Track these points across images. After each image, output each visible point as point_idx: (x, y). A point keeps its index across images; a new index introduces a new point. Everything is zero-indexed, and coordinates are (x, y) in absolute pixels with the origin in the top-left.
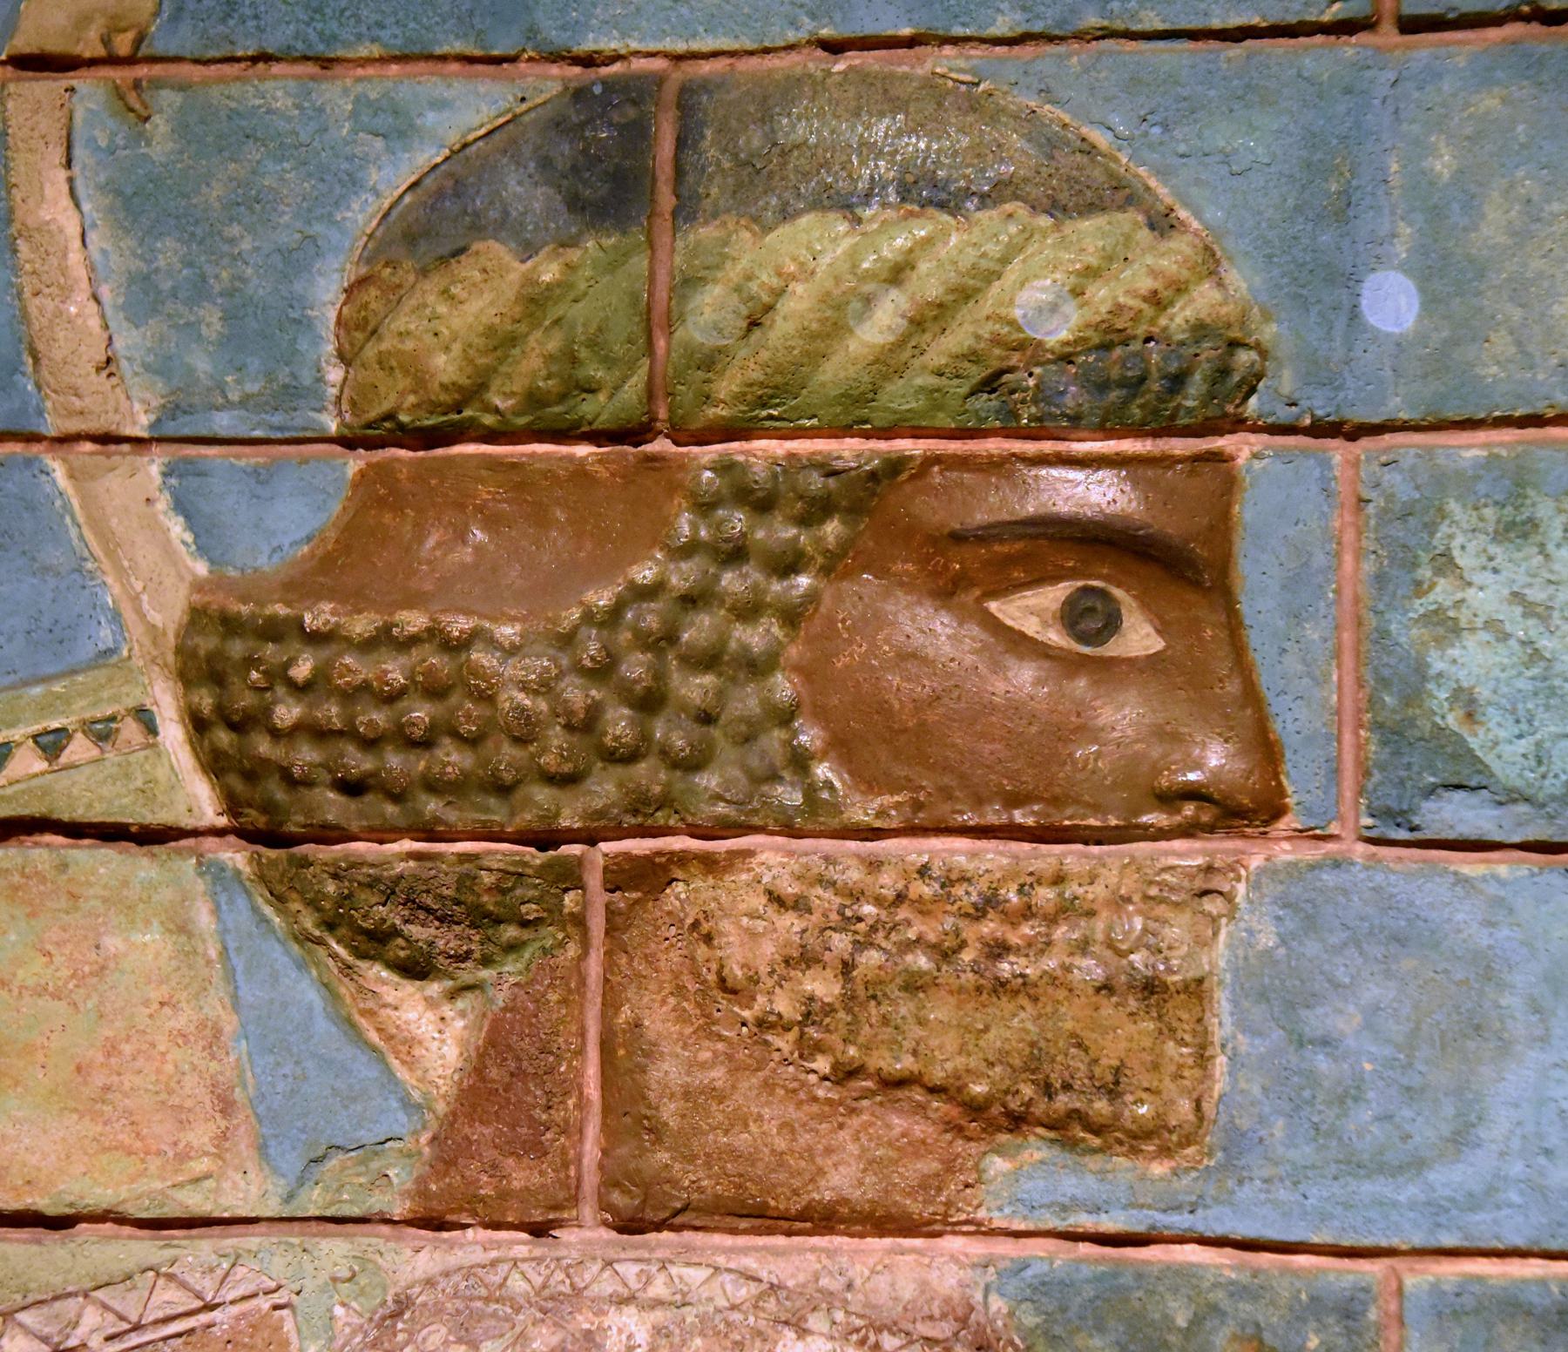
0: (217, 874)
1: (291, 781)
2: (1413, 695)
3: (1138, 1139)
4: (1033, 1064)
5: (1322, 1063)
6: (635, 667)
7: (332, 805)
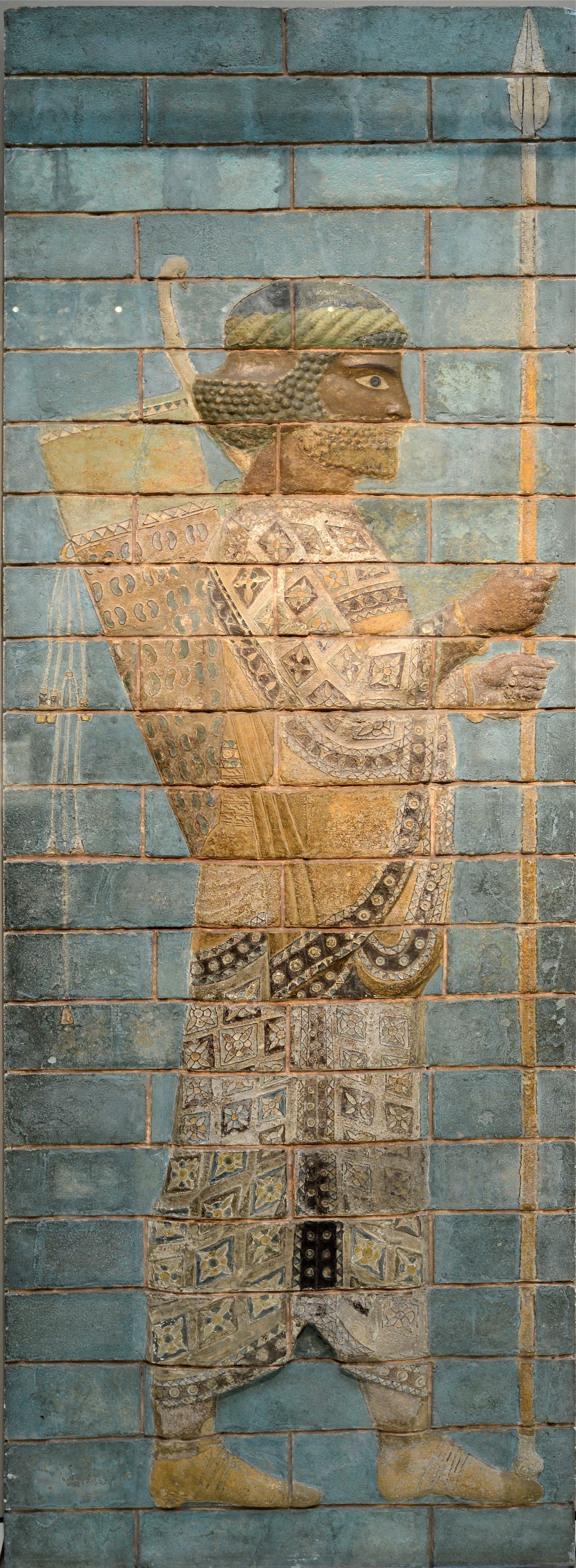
1: (218, 411)
2: (435, 396)
3: (383, 476)
4: (364, 463)
5: (418, 462)
6: (289, 391)
7: (227, 416)
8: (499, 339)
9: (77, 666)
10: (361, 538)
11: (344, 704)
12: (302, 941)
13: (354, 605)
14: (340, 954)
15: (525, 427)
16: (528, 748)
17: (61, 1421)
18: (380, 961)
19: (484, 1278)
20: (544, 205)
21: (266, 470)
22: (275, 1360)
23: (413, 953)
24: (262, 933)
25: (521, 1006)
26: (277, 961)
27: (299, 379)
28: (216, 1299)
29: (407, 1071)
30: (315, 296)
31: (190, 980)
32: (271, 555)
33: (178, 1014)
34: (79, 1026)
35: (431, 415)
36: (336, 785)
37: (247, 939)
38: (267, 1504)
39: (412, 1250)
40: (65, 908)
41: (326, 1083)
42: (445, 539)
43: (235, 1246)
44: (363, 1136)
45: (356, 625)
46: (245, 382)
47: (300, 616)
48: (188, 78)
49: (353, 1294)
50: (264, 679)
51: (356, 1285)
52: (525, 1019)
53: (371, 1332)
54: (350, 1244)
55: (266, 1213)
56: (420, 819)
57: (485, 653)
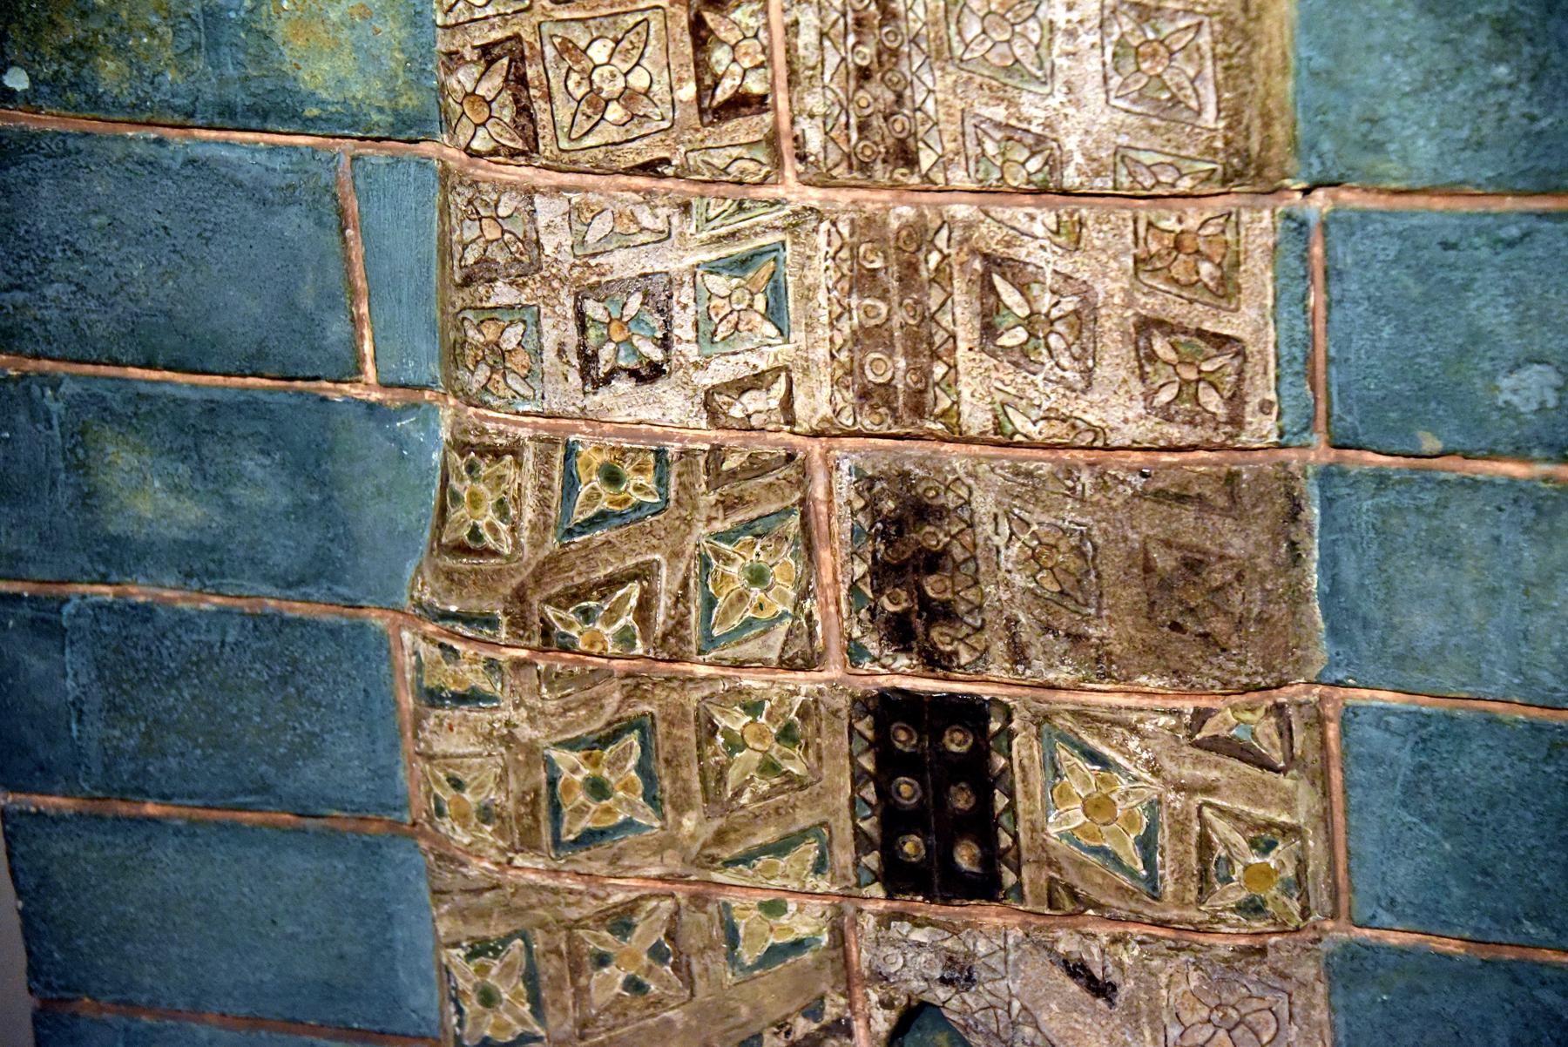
28: (619, 897)
39: (1259, 813)
41: (920, 234)
44: (1059, 429)
51: (1066, 900)
54: (1038, 777)
55: (750, 649)
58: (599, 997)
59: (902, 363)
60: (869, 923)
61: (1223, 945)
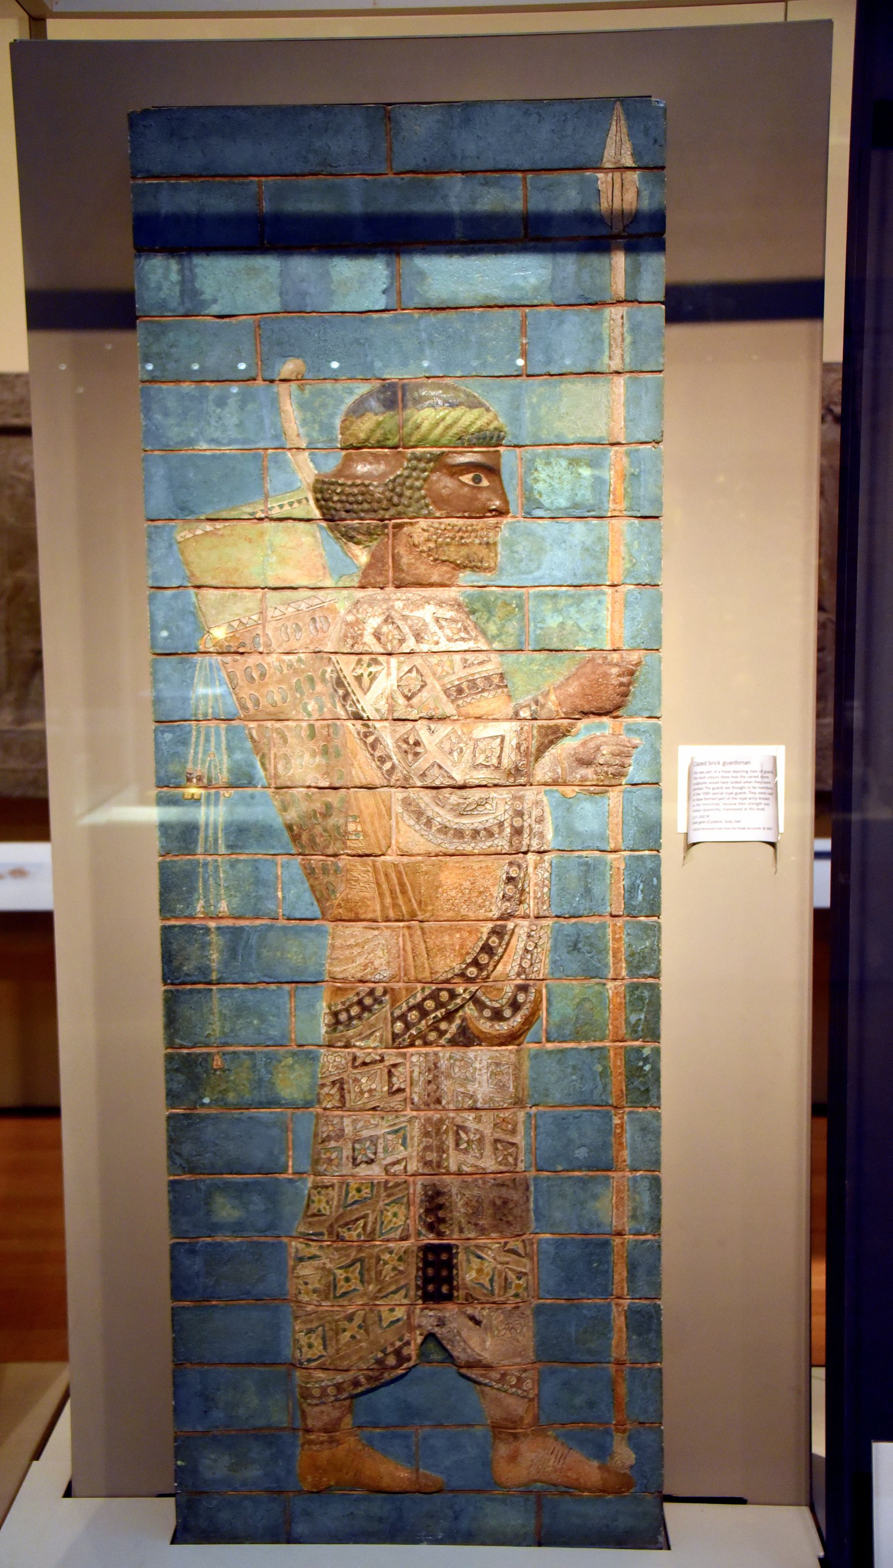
0: (321, 527)
1: (336, 510)
4: (468, 557)
6: (398, 490)
7: (343, 514)
8: (589, 436)
9: (218, 748)
10: (465, 629)
11: (451, 782)
12: (419, 995)
13: (460, 691)
14: (451, 1007)
15: (614, 521)
16: (616, 821)
17: (221, 1415)
18: (487, 1013)
19: (581, 1294)
20: (632, 301)
21: (380, 565)
22: (401, 1366)
23: (515, 1006)
24: (385, 988)
25: (612, 1053)
26: (397, 1013)
27: (408, 477)
28: (350, 1311)
29: (512, 1110)
30: (421, 397)
31: (324, 1030)
32: (384, 646)
33: (312, 1058)
34: (229, 1070)
35: (527, 510)
36: (445, 855)
37: (371, 992)
38: (398, 1489)
39: (519, 1269)
40: (214, 965)
41: (441, 1121)
42: (541, 628)
43: (366, 1265)
45: (462, 709)
46: (359, 482)
47: (411, 702)
48: (300, 179)
49: (468, 1308)
50: (382, 760)
51: (470, 1299)
52: (615, 1065)
53: (484, 1341)
54: (465, 1264)
55: (392, 1236)
56: (520, 885)
57: (577, 734)
58: (343, 1341)
59: (435, 1155)
60: (418, 1311)
61: (509, 1307)
